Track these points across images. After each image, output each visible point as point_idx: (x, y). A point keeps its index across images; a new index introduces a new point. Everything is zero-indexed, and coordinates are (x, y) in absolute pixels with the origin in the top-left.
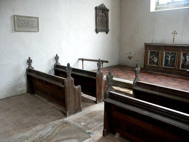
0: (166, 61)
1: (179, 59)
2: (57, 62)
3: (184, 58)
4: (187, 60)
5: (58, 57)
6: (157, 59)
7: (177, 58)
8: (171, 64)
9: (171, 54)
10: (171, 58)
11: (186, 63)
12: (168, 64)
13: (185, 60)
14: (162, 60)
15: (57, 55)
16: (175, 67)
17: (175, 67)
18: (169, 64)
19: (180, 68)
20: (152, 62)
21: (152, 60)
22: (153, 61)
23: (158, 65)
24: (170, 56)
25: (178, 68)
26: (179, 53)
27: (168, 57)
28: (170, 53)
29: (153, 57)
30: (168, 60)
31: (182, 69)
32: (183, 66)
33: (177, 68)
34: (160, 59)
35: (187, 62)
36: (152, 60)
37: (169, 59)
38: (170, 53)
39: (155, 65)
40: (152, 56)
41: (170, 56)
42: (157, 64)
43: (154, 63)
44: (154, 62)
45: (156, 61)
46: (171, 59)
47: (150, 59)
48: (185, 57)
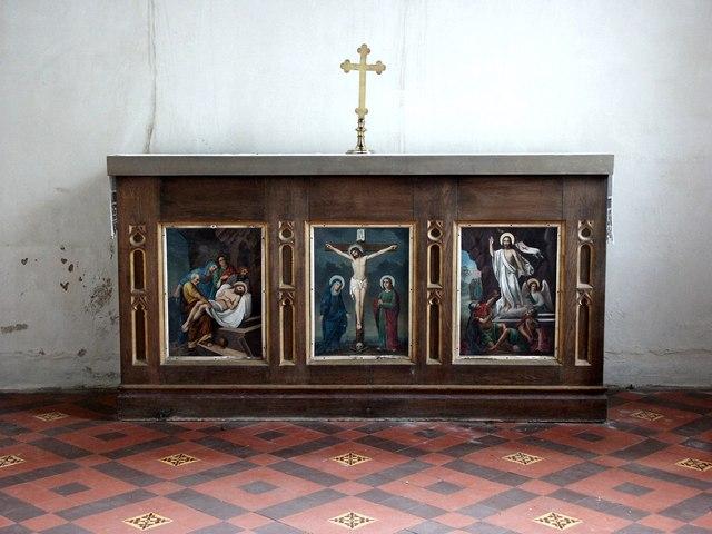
0: (334, 309)
1: (435, 280)
3: (475, 273)
6: (245, 300)
7: (421, 276)
8: (372, 333)
9: (367, 247)
10: (371, 276)
11: (494, 303)
12: (350, 332)
13: (489, 284)
17: (411, 349)
18: (361, 334)
19: (457, 358)
20: (199, 330)
21: (194, 314)
22: (210, 325)
24: (359, 265)
26: (435, 233)
27: (348, 273)
28: (361, 236)
29: (208, 288)
30: (344, 298)
32: (476, 337)
34: (272, 293)
35: (500, 303)
36: (194, 314)
37: (357, 286)
38: (361, 236)
39: (230, 357)
40: (195, 276)
41: (359, 265)
43: (221, 337)
44: (214, 326)
45: (233, 319)
46: (372, 291)
47: (180, 307)
48: (485, 262)
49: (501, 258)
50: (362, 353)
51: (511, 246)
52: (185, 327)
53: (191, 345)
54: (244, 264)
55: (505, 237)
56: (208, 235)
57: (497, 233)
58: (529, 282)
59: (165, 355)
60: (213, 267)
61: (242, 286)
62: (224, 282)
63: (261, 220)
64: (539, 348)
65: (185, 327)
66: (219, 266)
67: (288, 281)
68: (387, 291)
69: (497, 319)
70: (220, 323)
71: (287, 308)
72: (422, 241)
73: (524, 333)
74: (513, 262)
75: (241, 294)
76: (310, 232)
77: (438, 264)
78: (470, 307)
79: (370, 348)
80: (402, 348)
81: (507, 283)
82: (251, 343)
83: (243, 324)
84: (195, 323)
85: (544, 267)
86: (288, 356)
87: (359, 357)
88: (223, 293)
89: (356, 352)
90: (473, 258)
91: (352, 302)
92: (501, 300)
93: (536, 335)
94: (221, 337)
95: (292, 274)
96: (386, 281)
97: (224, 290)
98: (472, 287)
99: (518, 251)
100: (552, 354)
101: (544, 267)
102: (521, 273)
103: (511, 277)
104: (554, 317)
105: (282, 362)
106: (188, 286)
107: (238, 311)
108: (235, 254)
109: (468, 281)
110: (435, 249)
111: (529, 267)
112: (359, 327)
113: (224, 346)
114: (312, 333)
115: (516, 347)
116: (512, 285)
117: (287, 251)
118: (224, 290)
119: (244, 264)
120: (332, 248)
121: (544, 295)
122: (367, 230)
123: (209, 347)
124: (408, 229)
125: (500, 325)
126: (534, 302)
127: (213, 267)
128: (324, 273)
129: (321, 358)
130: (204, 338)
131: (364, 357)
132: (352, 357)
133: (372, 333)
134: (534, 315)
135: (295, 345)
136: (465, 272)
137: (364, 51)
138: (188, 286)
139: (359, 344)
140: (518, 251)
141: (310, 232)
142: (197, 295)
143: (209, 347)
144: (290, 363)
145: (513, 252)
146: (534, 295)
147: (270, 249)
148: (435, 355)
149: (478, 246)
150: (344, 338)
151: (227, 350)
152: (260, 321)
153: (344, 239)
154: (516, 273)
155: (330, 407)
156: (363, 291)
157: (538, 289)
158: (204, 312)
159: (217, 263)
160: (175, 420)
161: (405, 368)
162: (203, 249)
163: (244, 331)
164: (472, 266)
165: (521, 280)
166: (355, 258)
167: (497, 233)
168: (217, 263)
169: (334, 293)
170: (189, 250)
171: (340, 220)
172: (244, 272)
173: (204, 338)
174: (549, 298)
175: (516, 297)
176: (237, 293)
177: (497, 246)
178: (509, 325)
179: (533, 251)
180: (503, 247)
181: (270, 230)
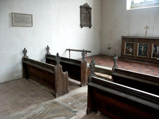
0: (140, 51)
1: (150, 49)
2: (48, 52)
3: (155, 49)
4: (158, 50)
5: (49, 48)
6: (132, 50)
7: (149, 49)
8: (144, 54)
9: (144, 46)
10: (144, 48)
11: (156, 53)
12: (141, 54)
13: (156, 50)
14: (136, 50)
15: (48, 46)
16: (147, 56)
17: (147, 56)
18: (142, 54)
19: (152, 57)
20: (128, 52)
21: (128, 50)
22: (129, 52)
23: (133, 55)
24: (143, 47)
25: (149, 57)
26: (151, 45)
27: (142, 48)
28: (143, 44)
29: (129, 48)
30: (141, 50)
31: (153, 58)
32: (154, 55)
33: (149, 57)
34: (134, 49)
35: (157, 52)
36: (128, 50)
37: (142, 49)
38: (143, 44)
39: (130, 55)
40: (128, 47)
41: (143, 47)
42: (132, 54)
43: (130, 53)
44: (129, 52)
45: (131, 51)
46: (144, 50)
47: (126, 50)
48: (156, 48)
54: (132, 46)
56: (130, 43)
57: (157, 45)
59: (125, 54)
72: (149, 45)
76: (138, 44)
77: (151, 48)
79: (143, 56)
82: (132, 54)
86: (135, 55)
90: (155, 47)
91: (142, 51)
94: (130, 53)
95: (136, 48)
105: (135, 56)
108: (132, 45)
114: (138, 53)
117: (136, 46)
119: (132, 46)
133: (144, 54)
137: (147, 26)
141: (138, 44)
153: (142, 45)
155: (138, 60)
160: (125, 60)
161: (146, 58)
167: (157, 45)
170: (128, 45)
171: (141, 43)
177: (157, 46)
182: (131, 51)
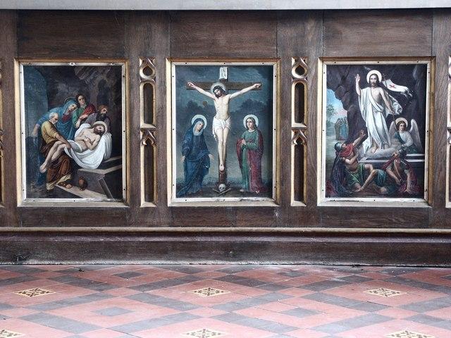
1: (300, 118)
3: (340, 112)
6: (104, 142)
7: (285, 115)
8: (235, 174)
9: (230, 86)
10: (235, 115)
11: (361, 143)
12: (213, 173)
13: (355, 124)
17: (276, 191)
18: (223, 176)
19: (322, 200)
21: (53, 154)
22: (68, 165)
24: (221, 104)
27: (210, 112)
28: (223, 74)
29: (67, 127)
30: (206, 140)
32: (341, 179)
34: (133, 131)
35: (367, 143)
36: (53, 154)
37: (220, 127)
38: (223, 74)
39: (91, 199)
40: (54, 115)
41: (221, 104)
42: (112, 185)
43: (81, 179)
44: (73, 167)
45: (93, 159)
46: (235, 131)
47: (38, 147)
48: (350, 100)
49: (368, 97)
50: (225, 195)
51: (378, 84)
52: (43, 168)
53: (49, 187)
55: (373, 75)
56: (67, 73)
58: (397, 121)
59: (22, 199)
60: (72, 106)
61: (102, 125)
62: (83, 121)
63: (122, 58)
64: (408, 190)
65: (43, 168)
66: (79, 106)
67: (149, 120)
68: (250, 131)
69: (364, 160)
70: (79, 163)
71: (149, 147)
72: (287, 77)
73: (392, 174)
74: (380, 101)
75: (101, 134)
76: (170, 70)
78: (336, 147)
79: (233, 190)
80: (266, 190)
81: (374, 122)
82: (112, 185)
83: (103, 165)
84: (54, 165)
85: (414, 106)
86: (150, 198)
87: (222, 199)
88: (82, 133)
89: (218, 194)
90: (339, 97)
91: (214, 142)
92: (368, 140)
93: (404, 177)
94: (81, 179)
96: (250, 120)
97: (84, 131)
98: (338, 127)
99: (385, 89)
100: (421, 196)
101: (414, 106)
102: (388, 112)
103: (379, 117)
104: (423, 158)
105: (144, 203)
106: (46, 125)
107: (97, 151)
108: (95, 92)
109: (334, 120)
110: (300, 87)
111: (397, 106)
112: (222, 168)
113: (84, 187)
114: (173, 172)
115: (383, 189)
116: (380, 125)
117: (148, 88)
118: (84, 131)
120: (194, 87)
121: (412, 134)
122: (230, 68)
123: (68, 189)
124: (271, 67)
125: (366, 166)
126: (402, 142)
127: (72, 106)
128: (187, 111)
129: (182, 200)
130: (63, 179)
131: (227, 199)
132: (214, 199)
133: (235, 174)
134: (403, 155)
135: (155, 187)
136: (330, 111)
138: (46, 125)
139: (222, 186)
140: (385, 89)
142: (56, 135)
143: (68, 189)
144: (151, 205)
145: (381, 90)
146: (403, 135)
147: (131, 87)
148: (299, 197)
149: (343, 81)
150: (206, 179)
151: (87, 191)
152: (120, 162)
153: (205, 77)
154: (384, 112)
155: (192, 250)
156: (226, 131)
157: (406, 129)
158: (63, 153)
159: (76, 101)
160: (32, 263)
161: (269, 210)
162: (62, 87)
163: (103, 172)
164: (338, 105)
165: (389, 119)
166: (218, 96)
167: (363, 71)
168: (76, 101)
169: (196, 133)
171: (201, 58)
172: (104, 111)
173: (63, 179)
174: (418, 137)
175: (383, 138)
176: (97, 132)
177: (364, 84)
178: (376, 166)
179: (401, 89)
180: (370, 85)
181: (131, 67)
182: (93, 159)
